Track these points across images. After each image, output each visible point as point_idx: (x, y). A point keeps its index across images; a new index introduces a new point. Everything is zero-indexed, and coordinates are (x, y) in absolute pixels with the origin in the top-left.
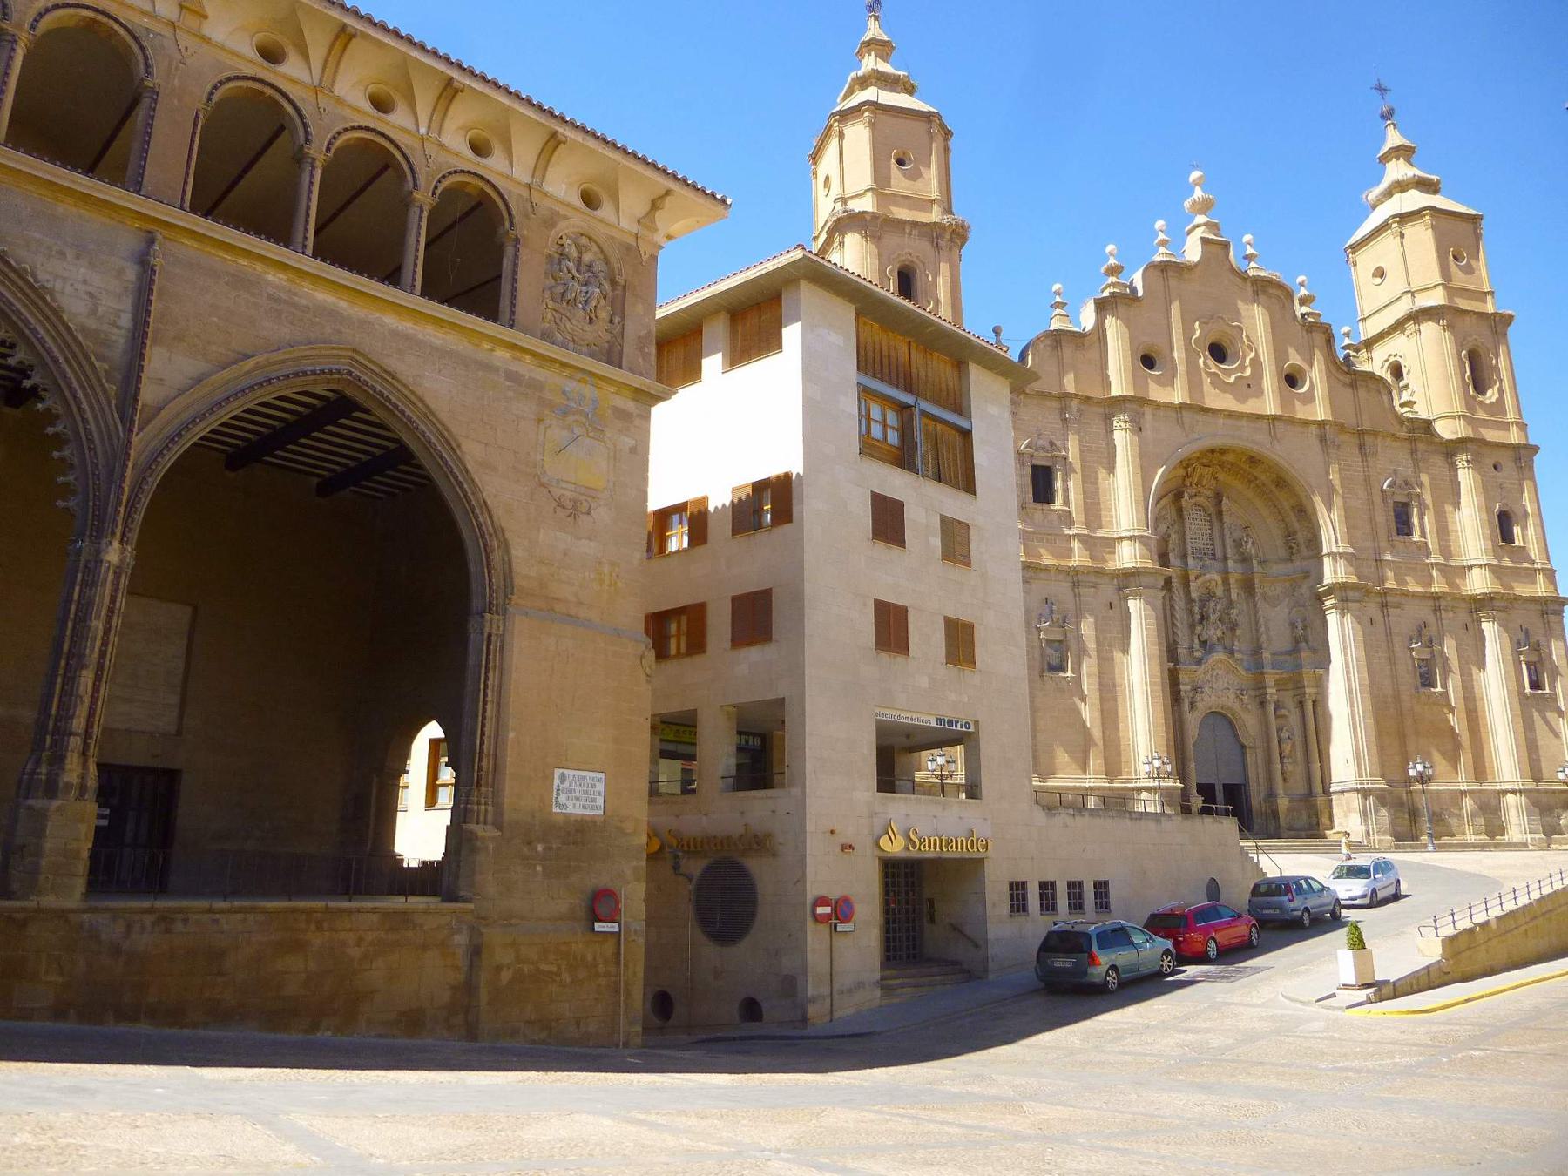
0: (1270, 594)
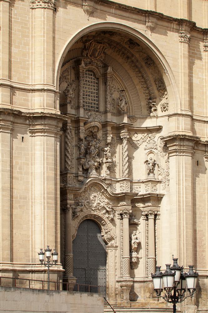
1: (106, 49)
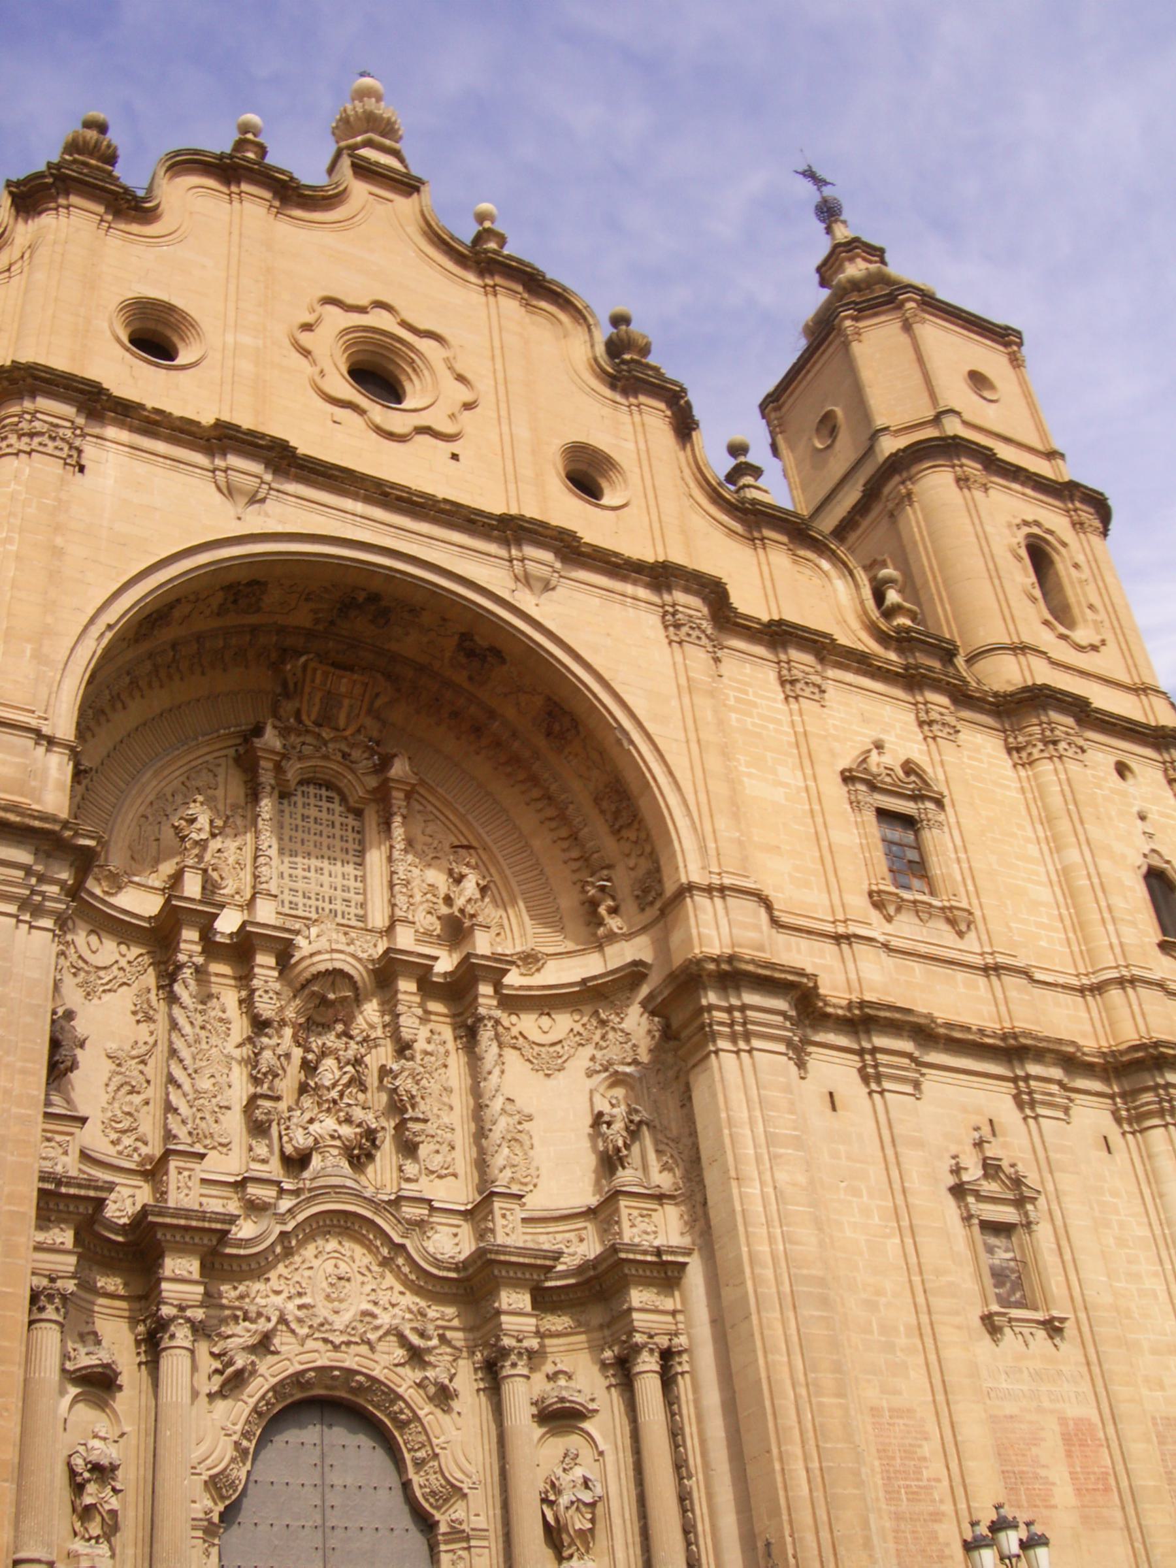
1: (377, 695)
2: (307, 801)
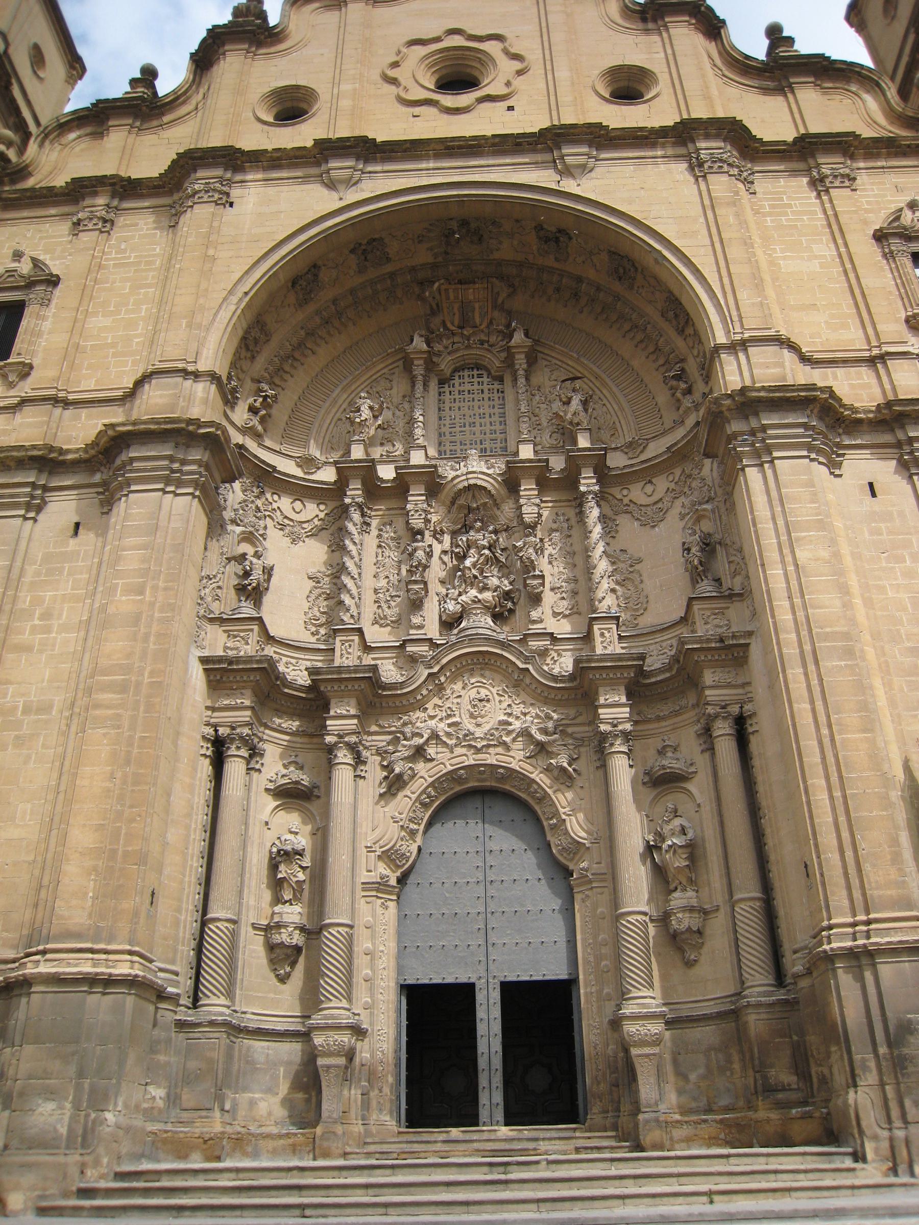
0: (643, 500)
1: (498, 293)
2: (462, 381)
